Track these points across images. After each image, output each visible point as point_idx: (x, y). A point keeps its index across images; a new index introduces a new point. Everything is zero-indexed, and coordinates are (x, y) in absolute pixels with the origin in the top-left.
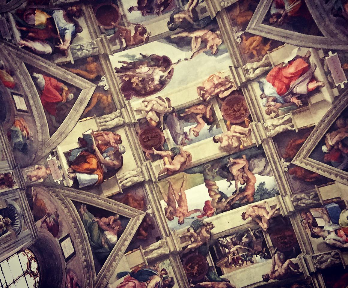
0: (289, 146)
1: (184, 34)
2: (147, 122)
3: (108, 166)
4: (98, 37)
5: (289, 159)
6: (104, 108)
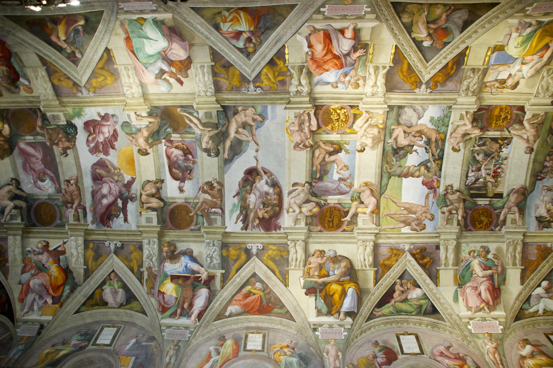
1: (228, 144)
2: (311, 216)
3: (344, 274)
4: (203, 236)
5: (418, 83)
6: (282, 256)
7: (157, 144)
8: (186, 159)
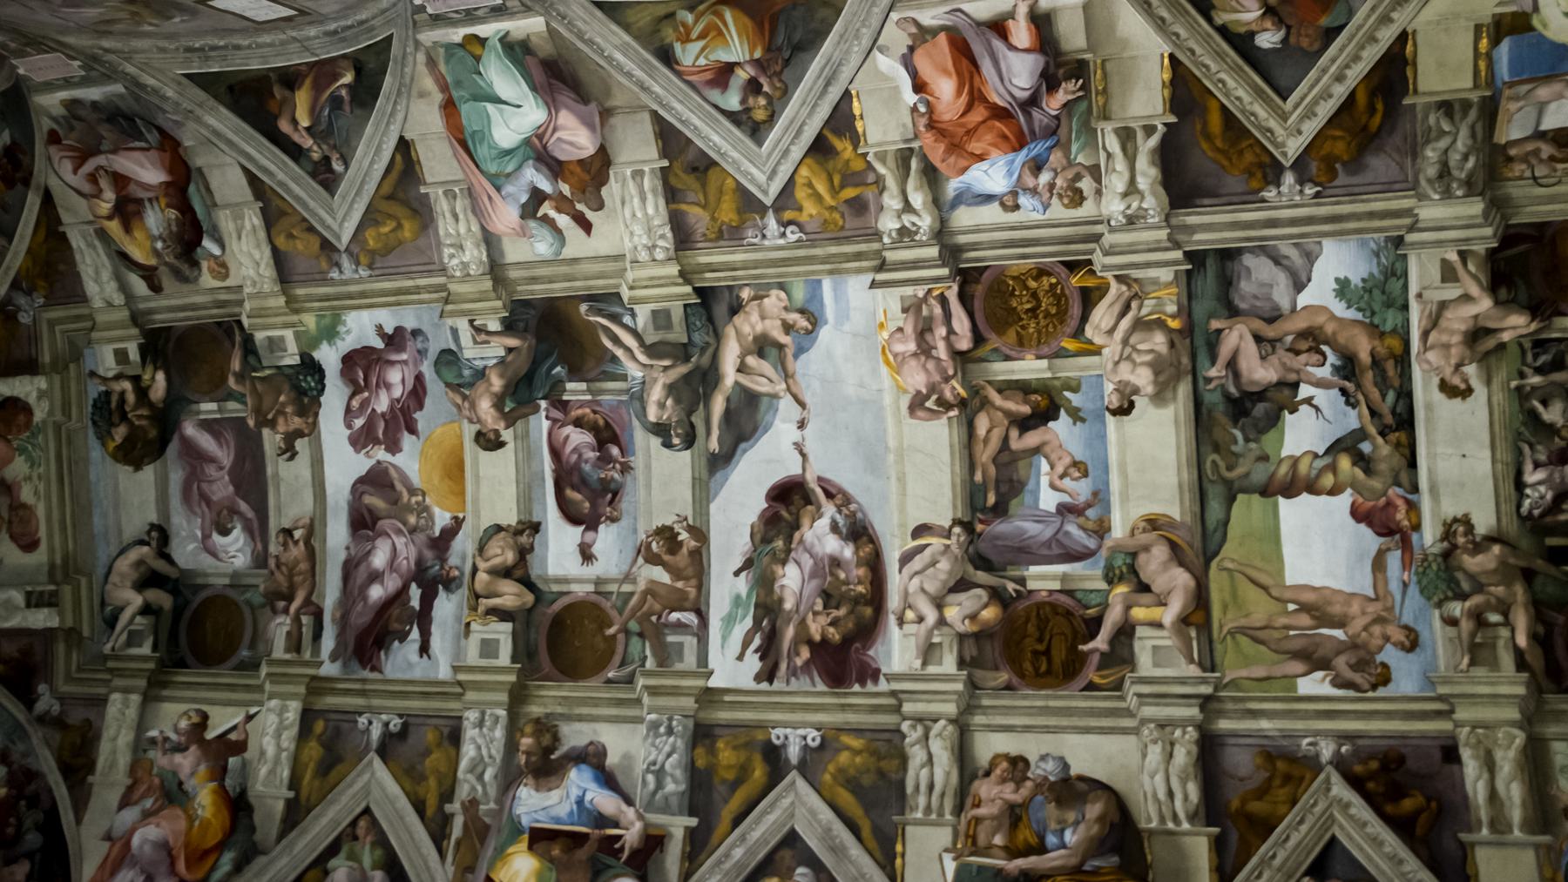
0: (1220, 157)
1: (718, 405)
2: (977, 636)
4: (638, 701)
5: (1271, 171)
7: (526, 416)
8: (605, 459)
